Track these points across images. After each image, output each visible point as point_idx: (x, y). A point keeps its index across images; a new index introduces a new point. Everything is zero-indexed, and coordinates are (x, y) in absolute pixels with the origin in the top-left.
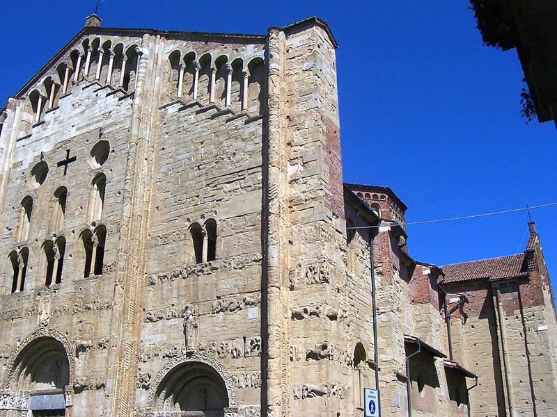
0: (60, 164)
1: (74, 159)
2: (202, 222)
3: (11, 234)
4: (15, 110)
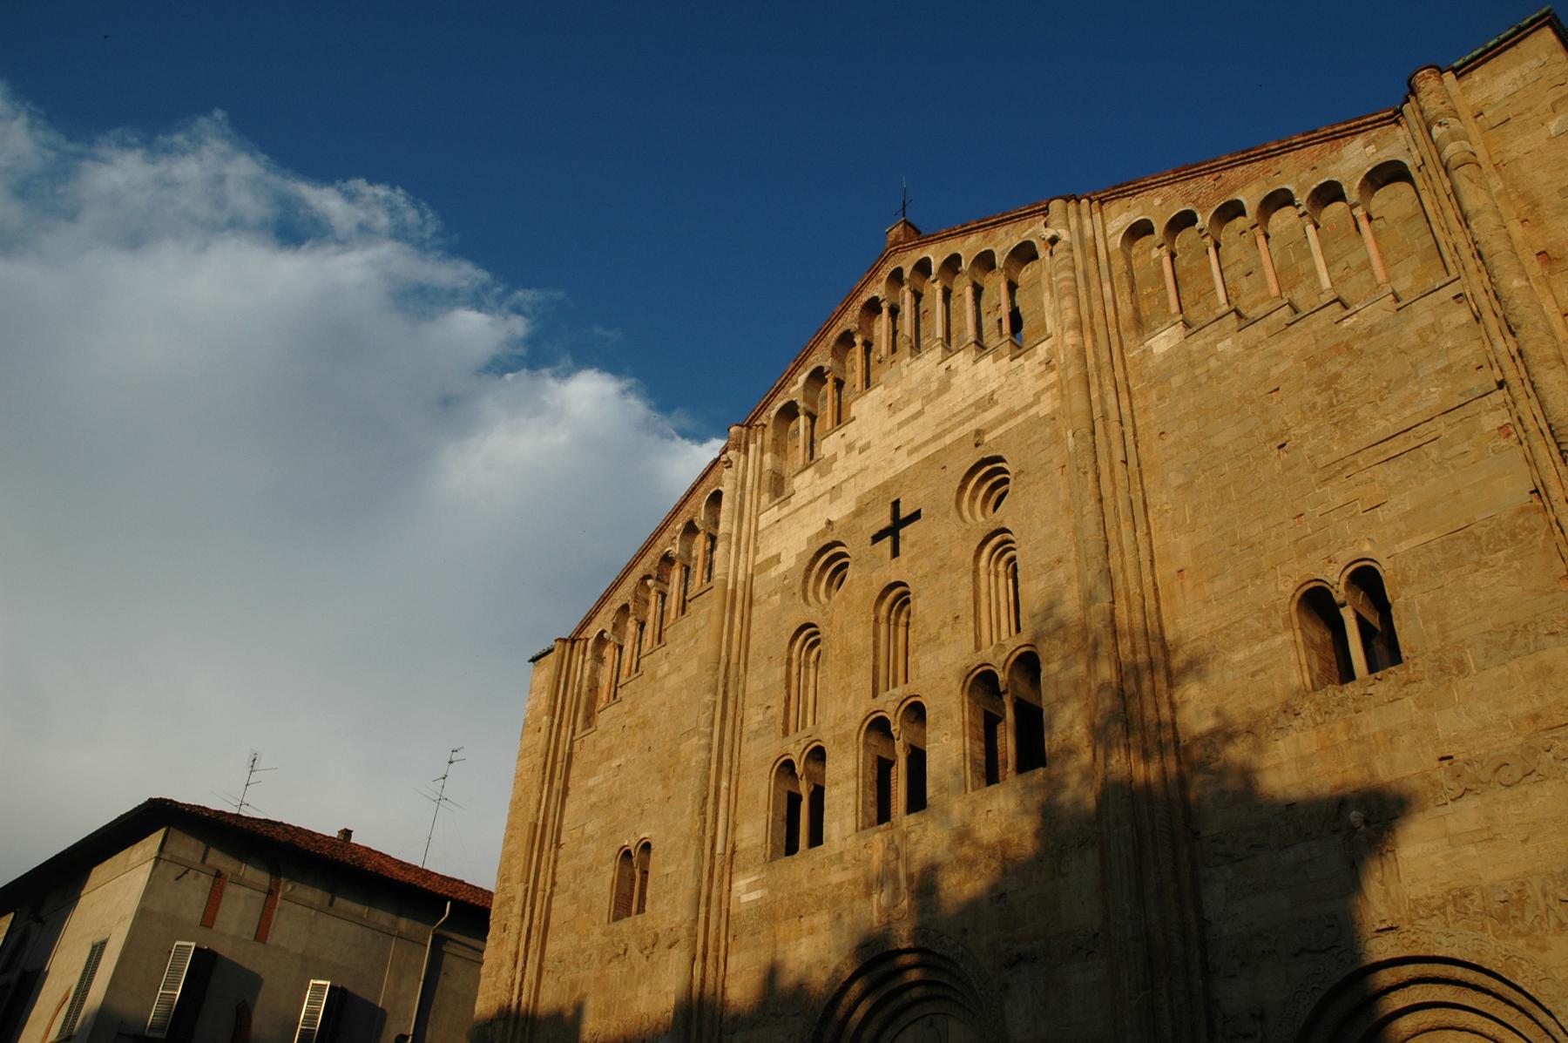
0: (877, 538)
1: (916, 516)
2: (1335, 578)
3: (772, 717)
4: (746, 452)
